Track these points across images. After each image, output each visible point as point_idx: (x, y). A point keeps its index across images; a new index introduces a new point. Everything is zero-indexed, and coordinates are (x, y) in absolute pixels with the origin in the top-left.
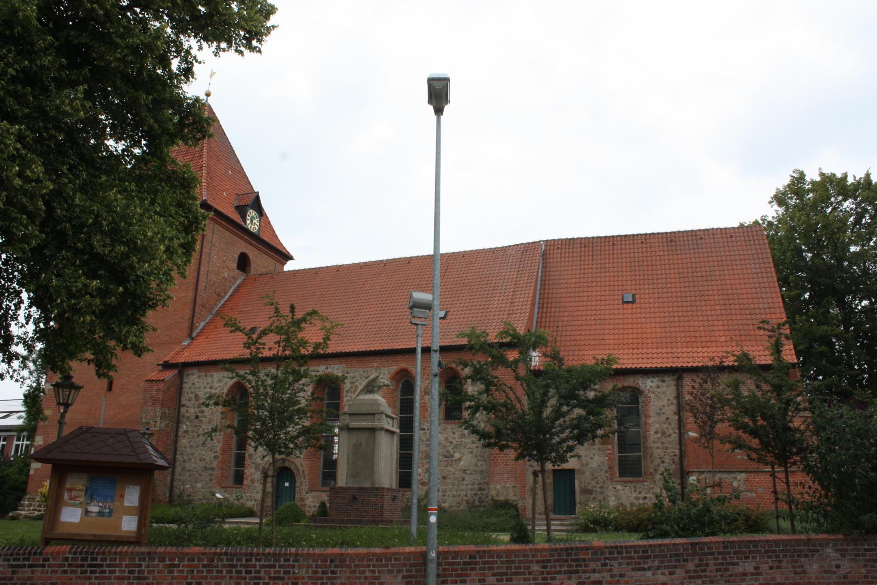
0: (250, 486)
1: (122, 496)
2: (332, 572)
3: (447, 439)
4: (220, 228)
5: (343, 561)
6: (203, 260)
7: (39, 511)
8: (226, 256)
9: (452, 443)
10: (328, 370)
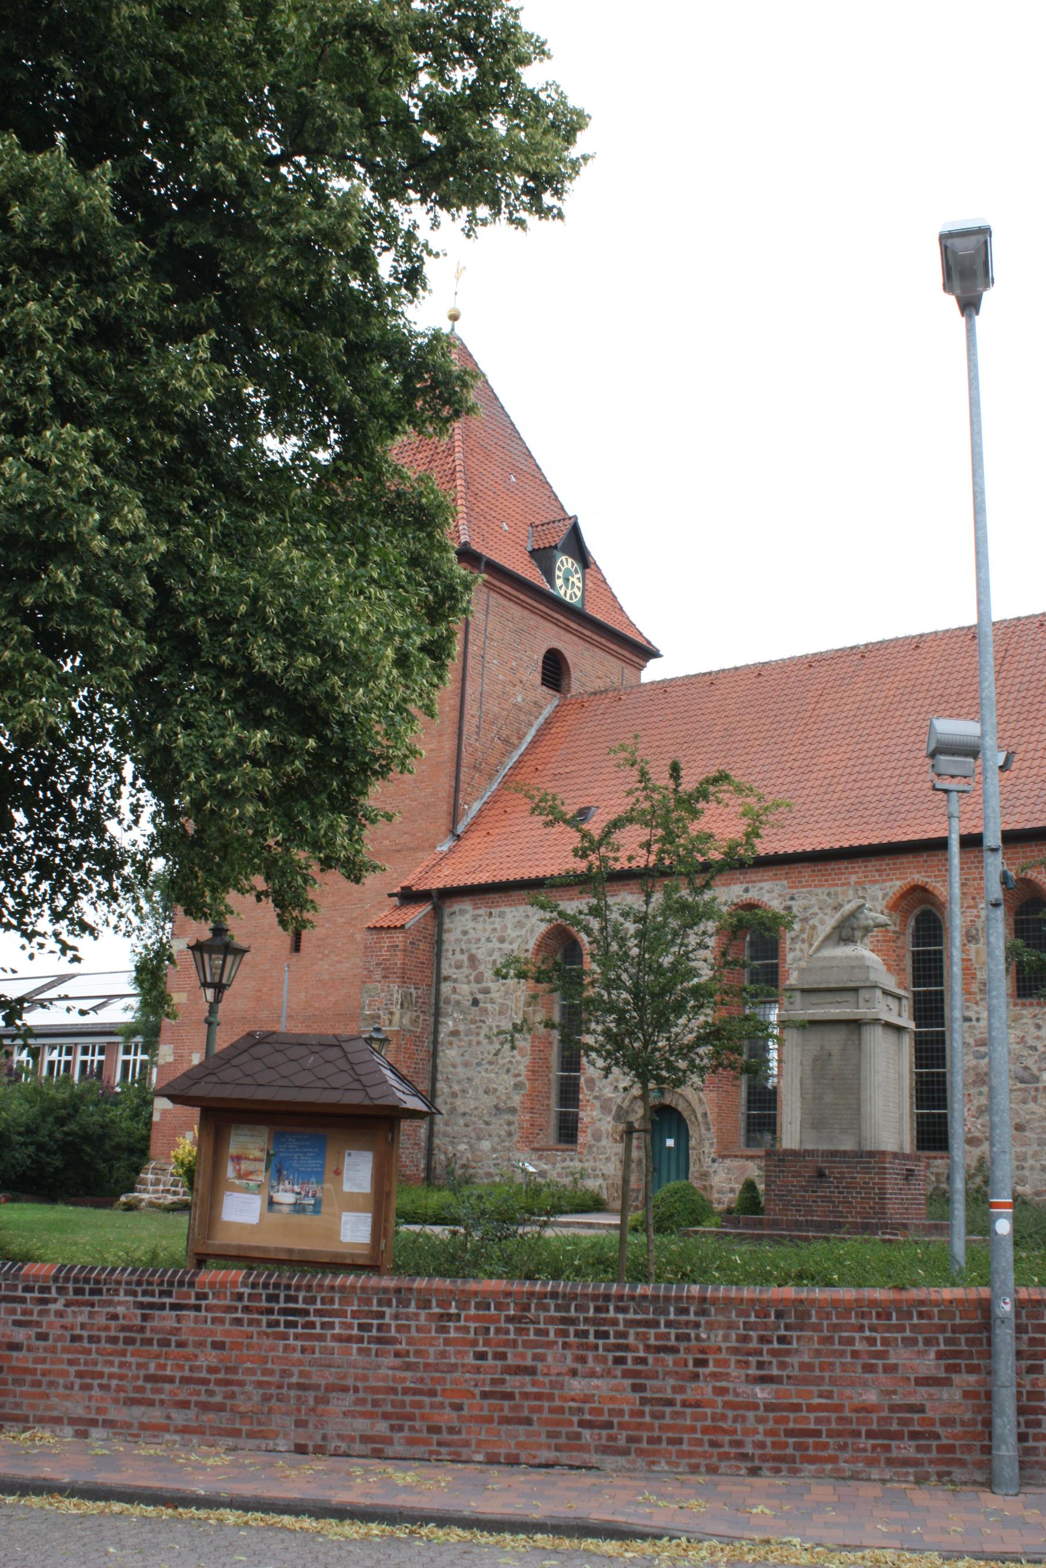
0: (591, 1147)
1: (338, 1172)
2: (782, 1340)
3: (1022, 1040)
5: (803, 1315)
6: (470, 671)
7: (175, 1193)
8: (516, 659)
9: (1035, 1049)
10: (749, 895)
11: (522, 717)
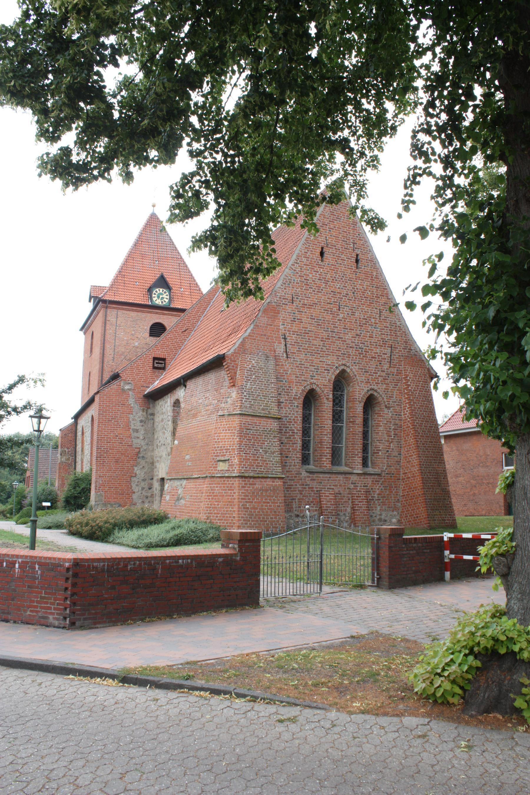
4: (124, 312)
8: (134, 330)
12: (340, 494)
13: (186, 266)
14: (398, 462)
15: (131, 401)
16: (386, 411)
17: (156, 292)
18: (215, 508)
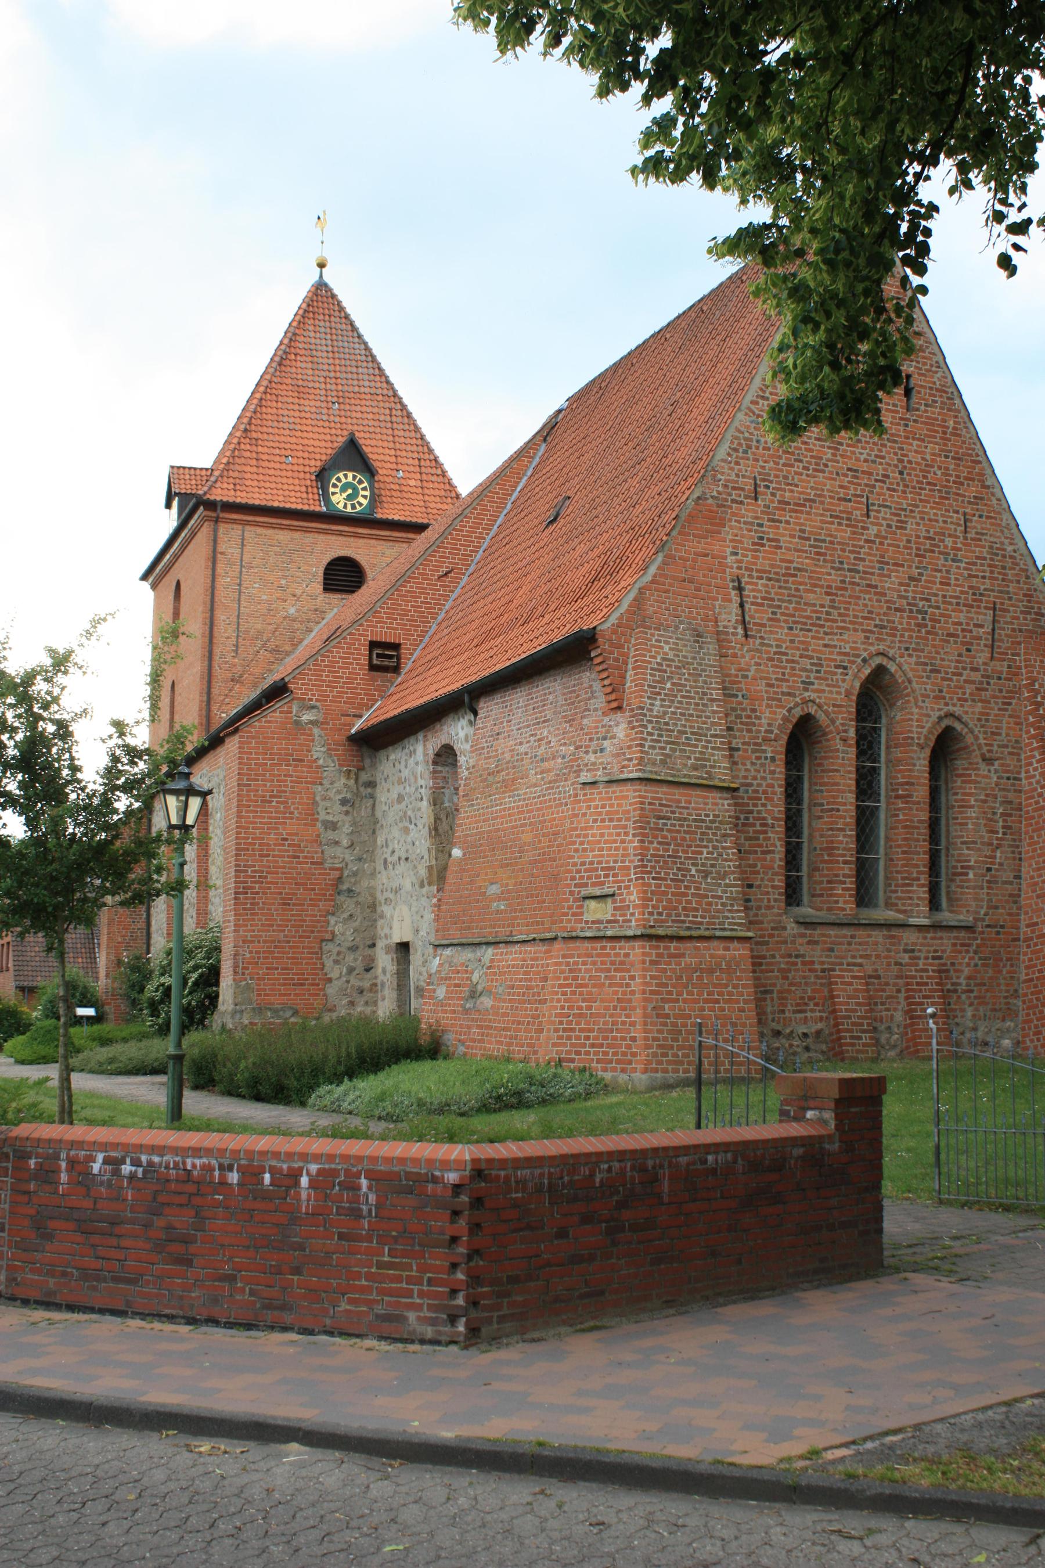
8: (285, 577)
11: (297, 626)
12: (878, 977)
13: (409, 415)
14: (1015, 897)
15: (318, 752)
16: (983, 768)
17: (339, 480)
18: (580, 1015)
